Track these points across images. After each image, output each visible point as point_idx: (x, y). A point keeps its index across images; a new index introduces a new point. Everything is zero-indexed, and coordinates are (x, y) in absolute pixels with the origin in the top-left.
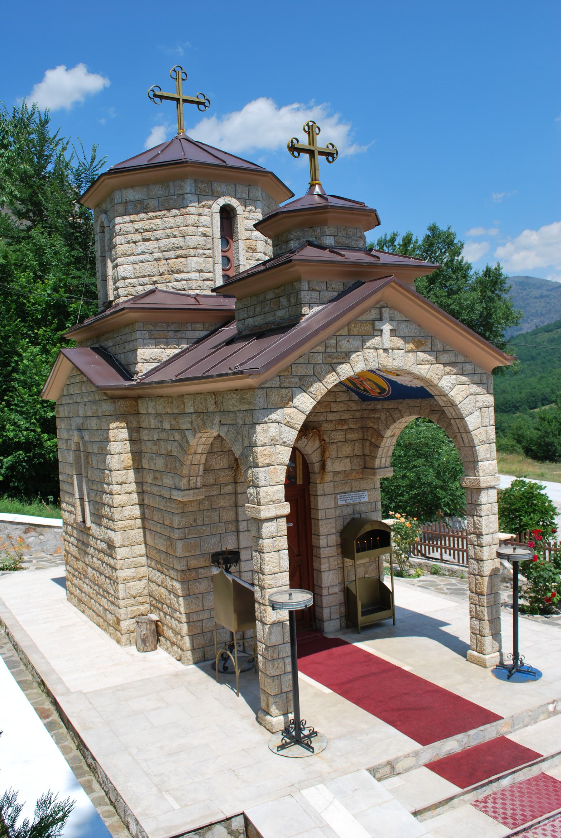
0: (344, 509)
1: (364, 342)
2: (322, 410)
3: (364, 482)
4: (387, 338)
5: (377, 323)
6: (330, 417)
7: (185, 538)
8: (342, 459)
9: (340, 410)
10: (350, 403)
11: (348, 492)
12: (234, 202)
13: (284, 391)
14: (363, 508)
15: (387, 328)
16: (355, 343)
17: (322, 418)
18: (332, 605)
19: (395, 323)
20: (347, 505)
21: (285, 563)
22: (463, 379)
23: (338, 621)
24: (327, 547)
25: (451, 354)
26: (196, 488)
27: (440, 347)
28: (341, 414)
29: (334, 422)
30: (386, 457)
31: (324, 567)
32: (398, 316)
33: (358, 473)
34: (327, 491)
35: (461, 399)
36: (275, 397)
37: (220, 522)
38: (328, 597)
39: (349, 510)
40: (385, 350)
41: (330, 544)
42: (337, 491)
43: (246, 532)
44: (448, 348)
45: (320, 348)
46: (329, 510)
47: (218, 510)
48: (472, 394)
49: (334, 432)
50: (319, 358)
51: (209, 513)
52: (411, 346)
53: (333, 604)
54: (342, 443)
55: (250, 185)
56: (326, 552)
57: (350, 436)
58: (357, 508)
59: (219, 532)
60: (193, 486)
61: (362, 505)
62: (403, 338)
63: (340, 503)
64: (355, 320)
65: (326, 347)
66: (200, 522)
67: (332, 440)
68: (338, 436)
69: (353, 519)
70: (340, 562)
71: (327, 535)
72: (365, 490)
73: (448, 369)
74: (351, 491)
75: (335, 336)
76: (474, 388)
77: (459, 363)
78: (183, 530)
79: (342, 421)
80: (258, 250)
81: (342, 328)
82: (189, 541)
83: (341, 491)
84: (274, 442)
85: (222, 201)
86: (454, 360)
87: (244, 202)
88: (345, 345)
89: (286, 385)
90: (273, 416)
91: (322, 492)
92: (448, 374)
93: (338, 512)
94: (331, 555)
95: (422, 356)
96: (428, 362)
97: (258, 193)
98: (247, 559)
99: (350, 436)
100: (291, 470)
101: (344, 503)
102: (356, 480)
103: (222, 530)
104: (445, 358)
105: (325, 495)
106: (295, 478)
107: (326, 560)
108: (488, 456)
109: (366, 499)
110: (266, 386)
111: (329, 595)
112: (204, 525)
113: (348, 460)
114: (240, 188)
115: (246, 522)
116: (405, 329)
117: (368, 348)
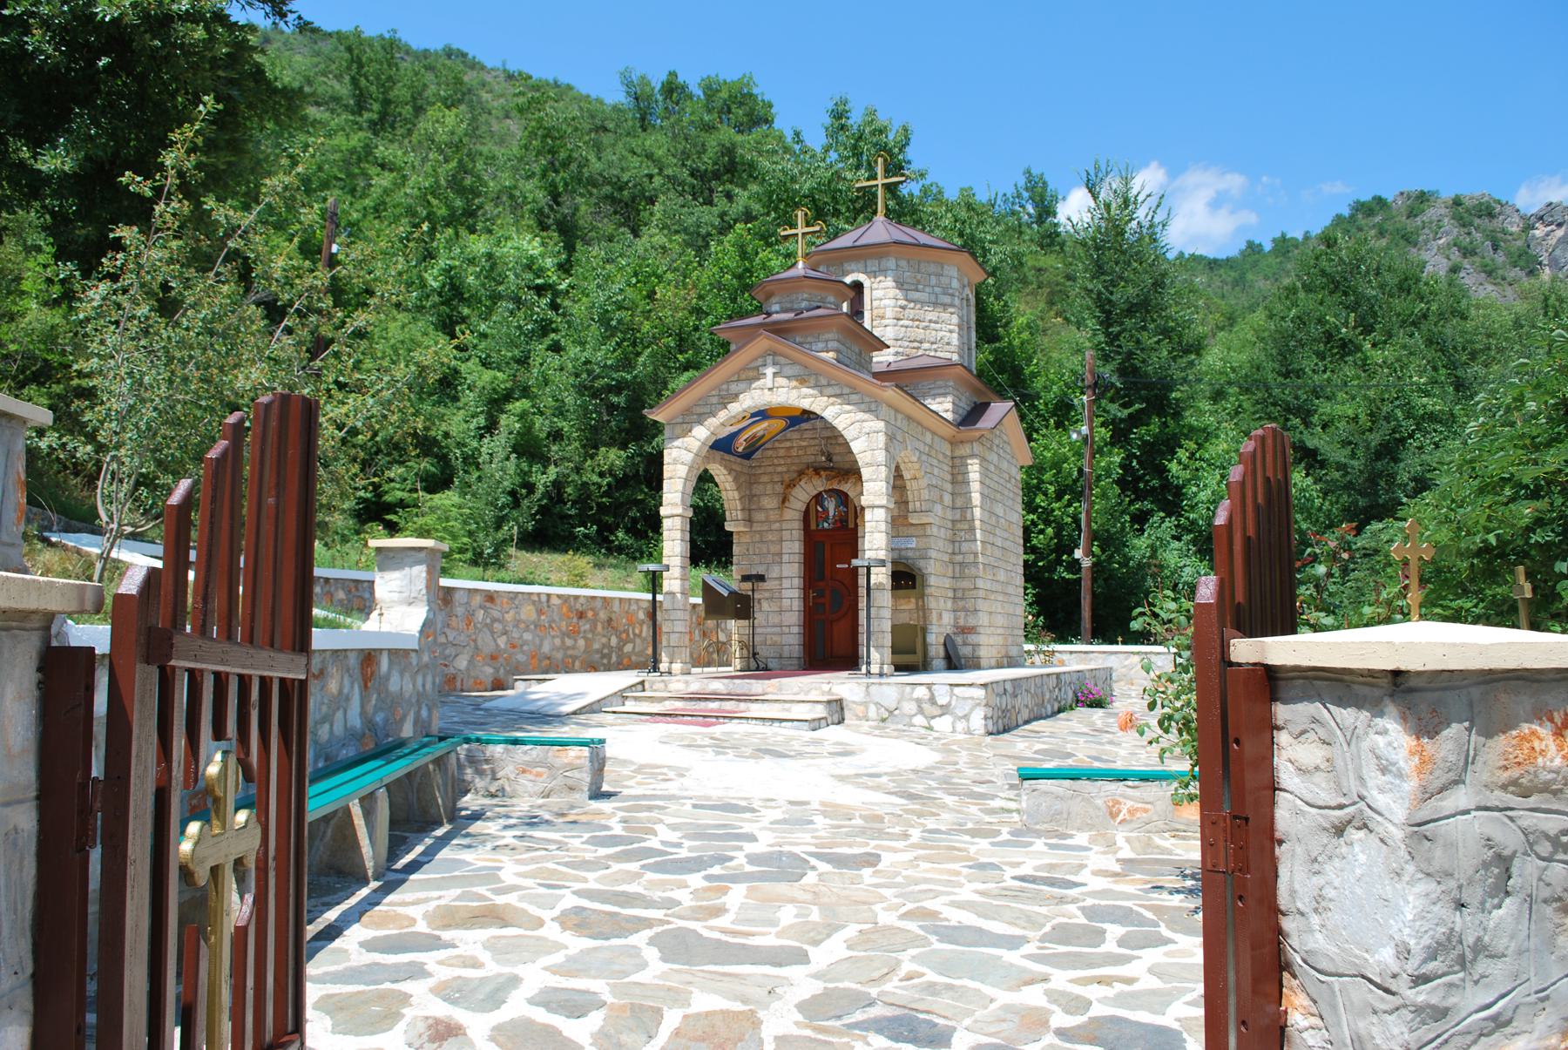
4: (768, 381)
12: (862, 277)
14: (910, 554)
15: (769, 371)
16: (742, 386)
27: (824, 382)
32: (782, 360)
36: (678, 430)
50: (715, 400)
52: (794, 383)
55: (880, 257)
62: (788, 378)
64: (744, 369)
73: (832, 400)
76: (861, 416)
84: (675, 462)
87: (873, 274)
88: (734, 388)
90: (676, 443)
95: (805, 391)
97: (891, 263)
104: (829, 391)
114: (869, 263)
116: (788, 370)
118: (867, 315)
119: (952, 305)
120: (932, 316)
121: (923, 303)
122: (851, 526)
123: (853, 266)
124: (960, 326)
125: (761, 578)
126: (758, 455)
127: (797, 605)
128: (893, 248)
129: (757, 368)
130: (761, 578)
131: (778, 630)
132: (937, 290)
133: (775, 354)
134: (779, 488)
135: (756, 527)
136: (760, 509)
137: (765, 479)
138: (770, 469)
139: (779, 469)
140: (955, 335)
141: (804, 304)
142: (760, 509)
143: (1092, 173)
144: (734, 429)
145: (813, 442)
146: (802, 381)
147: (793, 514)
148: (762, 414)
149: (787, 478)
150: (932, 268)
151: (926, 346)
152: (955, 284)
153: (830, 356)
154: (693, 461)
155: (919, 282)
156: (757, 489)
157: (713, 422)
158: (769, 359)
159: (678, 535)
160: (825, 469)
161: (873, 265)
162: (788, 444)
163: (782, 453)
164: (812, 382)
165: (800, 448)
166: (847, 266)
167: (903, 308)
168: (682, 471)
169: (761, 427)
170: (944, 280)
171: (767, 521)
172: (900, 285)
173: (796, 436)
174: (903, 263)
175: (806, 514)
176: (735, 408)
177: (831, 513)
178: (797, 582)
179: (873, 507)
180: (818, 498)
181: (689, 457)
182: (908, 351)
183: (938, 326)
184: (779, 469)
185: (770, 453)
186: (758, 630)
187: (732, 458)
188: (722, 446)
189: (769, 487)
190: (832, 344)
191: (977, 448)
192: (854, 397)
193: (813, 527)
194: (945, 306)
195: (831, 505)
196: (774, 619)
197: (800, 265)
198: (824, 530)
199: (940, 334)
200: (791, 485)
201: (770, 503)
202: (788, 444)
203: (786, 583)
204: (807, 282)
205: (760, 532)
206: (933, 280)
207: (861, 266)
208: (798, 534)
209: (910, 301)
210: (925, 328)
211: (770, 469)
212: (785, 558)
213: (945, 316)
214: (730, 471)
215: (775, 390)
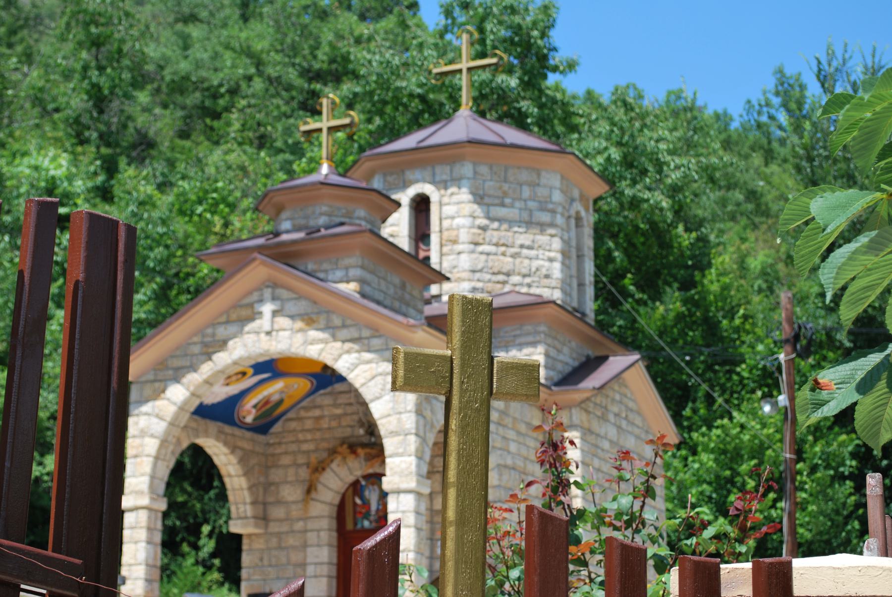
1: (243, 326)
5: (256, 306)
12: (428, 189)
13: (157, 385)
16: (232, 329)
19: (278, 303)
21: (125, 548)
22: (367, 356)
25: (352, 330)
27: (337, 321)
32: (284, 293)
35: (363, 381)
36: (148, 391)
40: (268, 333)
44: (349, 322)
45: (195, 339)
48: (381, 374)
50: (196, 349)
52: (299, 324)
55: (452, 161)
60: (243, 515)
62: (292, 317)
64: (236, 306)
65: (203, 336)
66: (266, 562)
73: (348, 345)
75: (214, 324)
77: (364, 338)
80: (461, 240)
81: (221, 315)
84: (143, 434)
85: (412, 191)
86: (356, 335)
87: (443, 185)
88: (221, 332)
89: (159, 378)
90: (146, 408)
92: (348, 352)
95: (313, 334)
96: (321, 341)
97: (467, 169)
104: (344, 333)
108: (401, 450)
110: (143, 379)
114: (438, 169)
116: (291, 307)
117: (248, 333)
118: (434, 238)
119: (552, 225)
120: (524, 238)
121: (511, 223)
123: (417, 174)
124: (565, 254)
126: (277, 428)
128: (469, 149)
129: (251, 305)
132: (532, 204)
133: (275, 285)
134: (304, 473)
135: (274, 527)
136: (279, 502)
138: (293, 447)
139: (305, 447)
140: (557, 266)
141: (322, 220)
142: (279, 502)
143: (824, 61)
144: (234, 389)
145: (349, 410)
146: (310, 321)
148: (270, 368)
149: (314, 458)
150: (524, 176)
151: (516, 279)
152: (557, 196)
153: (350, 288)
154: (167, 432)
155: (505, 194)
156: (276, 475)
157: (194, 378)
158: (267, 293)
159: (143, 534)
160: (364, 445)
161: (443, 172)
162: (317, 413)
163: (309, 424)
164: (322, 322)
166: (410, 175)
167: (484, 229)
168: (151, 445)
169: (275, 389)
170: (541, 192)
171: (287, 519)
172: (479, 198)
173: (327, 401)
174: (484, 170)
175: (341, 508)
176: (222, 359)
179: (398, 492)
181: (160, 427)
182: (490, 286)
183: (533, 253)
185: (293, 425)
187: (237, 432)
188: (217, 413)
189: (291, 471)
190: (353, 272)
191: (577, 416)
192: (376, 342)
193: (350, 526)
194: (542, 227)
197: (325, 169)
199: (535, 264)
200: (319, 468)
201: (291, 493)
202: (317, 413)
204: (326, 190)
205: (279, 535)
206: (526, 192)
207: (427, 173)
209: (492, 219)
210: (514, 256)
211: (293, 447)
212: (310, 570)
213: (543, 239)
214: (233, 449)
215: (274, 333)
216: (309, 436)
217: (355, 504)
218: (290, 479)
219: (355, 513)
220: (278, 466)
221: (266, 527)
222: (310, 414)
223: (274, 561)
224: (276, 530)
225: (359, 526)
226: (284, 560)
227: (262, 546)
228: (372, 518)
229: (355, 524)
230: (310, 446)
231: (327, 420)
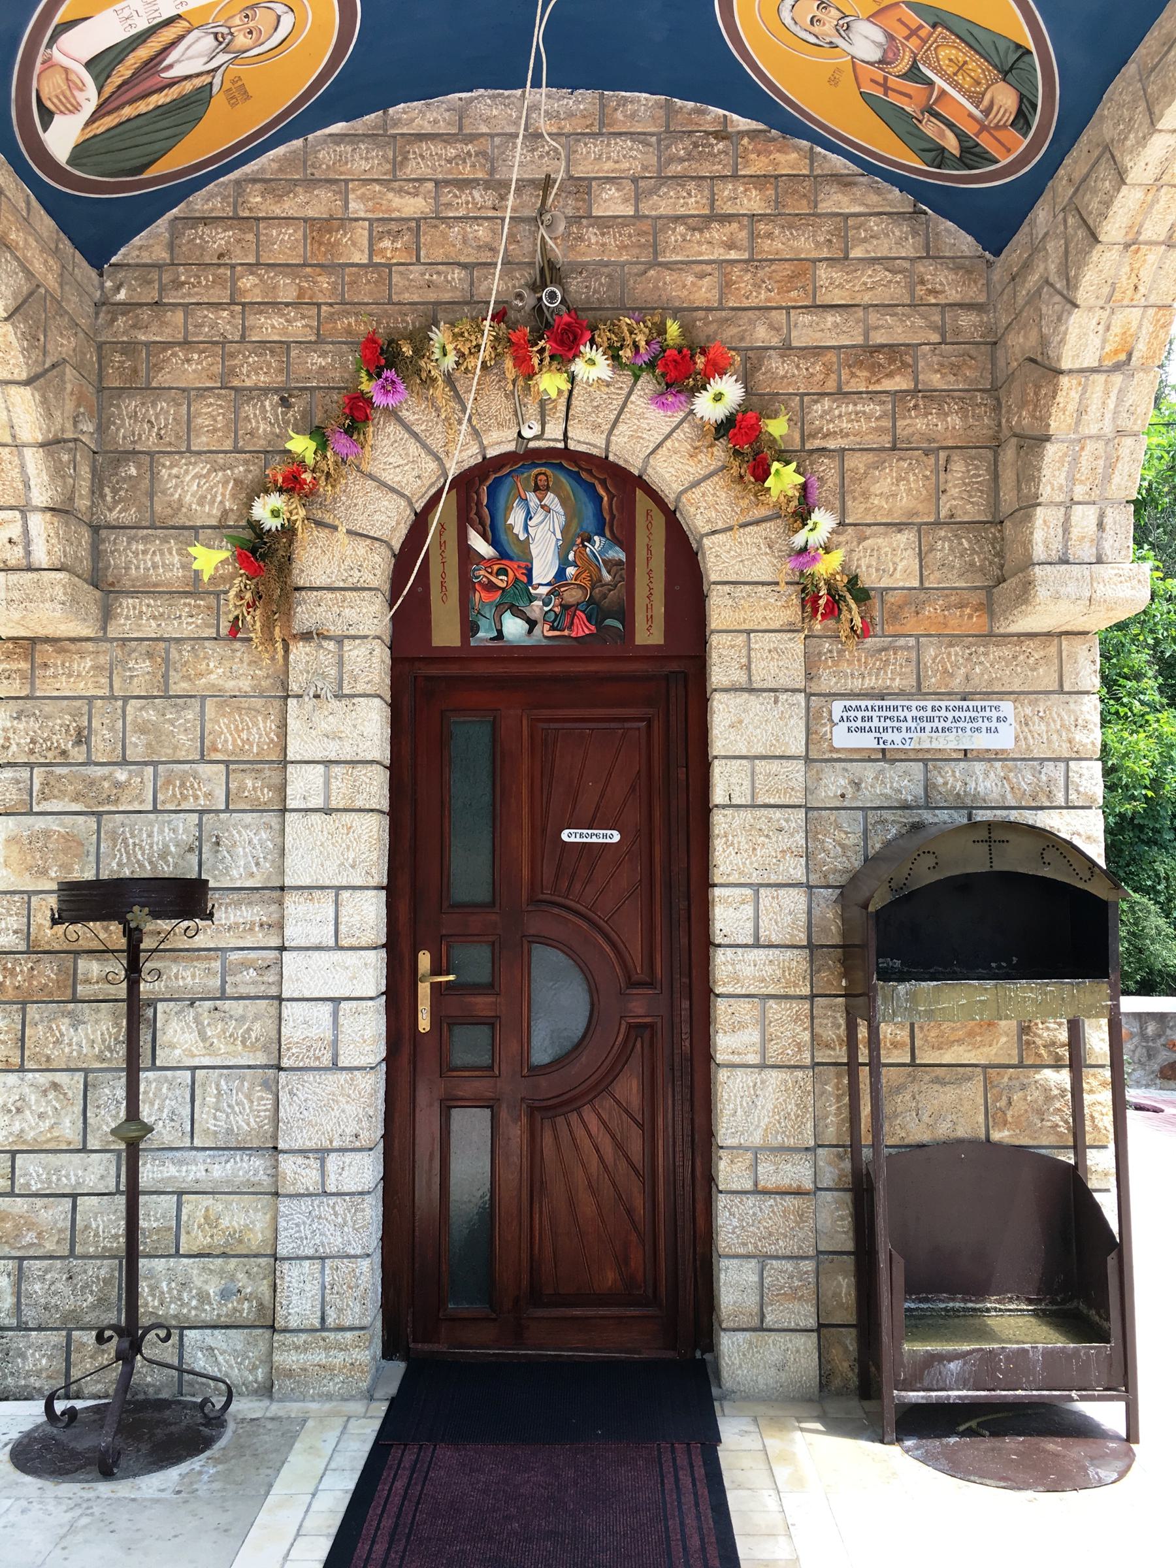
0: (868, 772)
2: (761, 297)
3: (995, 652)
6: (809, 330)
7: (31, 813)
8: (868, 531)
9: (867, 298)
10: (926, 269)
11: (901, 694)
14: (986, 783)
17: (762, 334)
18: (771, 1249)
20: (885, 755)
23: (807, 1344)
24: (757, 945)
26: (30, 569)
28: (873, 318)
29: (831, 357)
30: (1101, 503)
31: (733, 1038)
33: (961, 606)
34: (765, 671)
37: (203, 760)
38: (751, 1201)
39: (903, 782)
41: (770, 932)
42: (827, 681)
43: (316, 818)
46: (775, 766)
47: (196, 703)
49: (827, 402)
51: (151, 715)
53: (782, 1246)
54: (870, 457)
56: (749, 971)
57: (920, 424)
58: (951, 778)
59: (189, 804)
61: (979, 767)
63: (842, 738)
66: (102, 744)
67: (813, 436)
68: (848, 422)
69: (917, 827)
70: (833, 1027)
71: (756, 887)
72: (1003, 695)
74: (919, 692)
78: (25, 773)
79: (870, 356)
82: (40, 823)
83: (857, 685)
91: (740, 677)
93: (834, 784)
94: (771, 990)
98: (314, 941)
99: (917, 424)
100: (607, 577)
101: (867, 741)
102: (954, 639)
103: (209, 795)
105: (751, 690)
106: (625, 613)
107: (744, 1006)
109: (1004, 739)
111: (758, 1191)
112: (124, 762)
113: (905, 538)
115: (321, 768)
122: (649, 631)
125: (187, 898)
126: (147, 245)
127: (366, 1035)
130: (187, 898)
131: (253, 1168)
135: (136, 618)
137: (192, 370)
138: (225, 322)
139: (270, 326)
147: (345, 570)
156: (141, 423)
162: (320, 203)
165: (384, 226)
173: (364, 162)
177: (544, 569)
178: (368, 915)
180: (479, 491)
184: (270, 326)
185: (219, 239)
186: (148, 1173)
193: (445, 632)
195: (542, 530)
196: (237, 1110)
198: (503, 652)
202: (320, 203)
203: (306, 920)
205: (161, 649)
208: (371, 664)
211: (225, 322)
212: (304, 785)
216: (287, 289)
217: (467, 554)
218: (201, 442)
219: (466, 586)
220: (151, 392)
221: (107, 615)
222: (288, 207)
223: (137, 747)
224: (150, 629)
225: (485, 634)
226: (186, 744)
227: (85, 688)
228: (536, 609)
229: (469, 628)
230: (299, 328)
231: (361, 233)
